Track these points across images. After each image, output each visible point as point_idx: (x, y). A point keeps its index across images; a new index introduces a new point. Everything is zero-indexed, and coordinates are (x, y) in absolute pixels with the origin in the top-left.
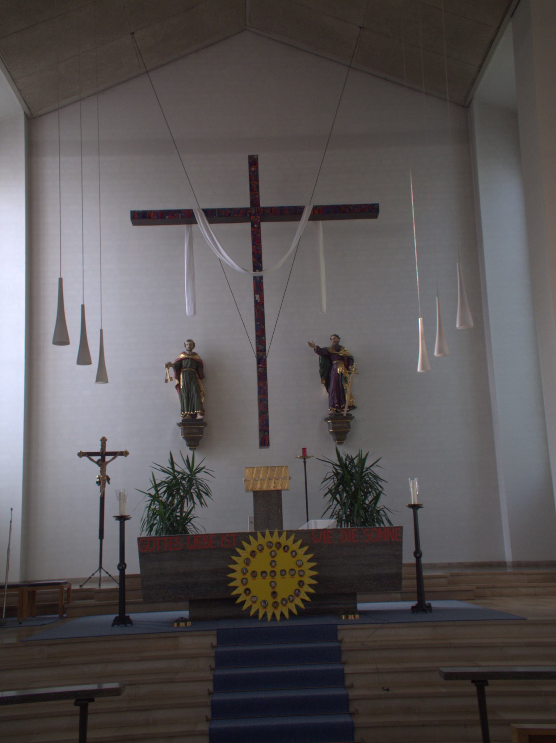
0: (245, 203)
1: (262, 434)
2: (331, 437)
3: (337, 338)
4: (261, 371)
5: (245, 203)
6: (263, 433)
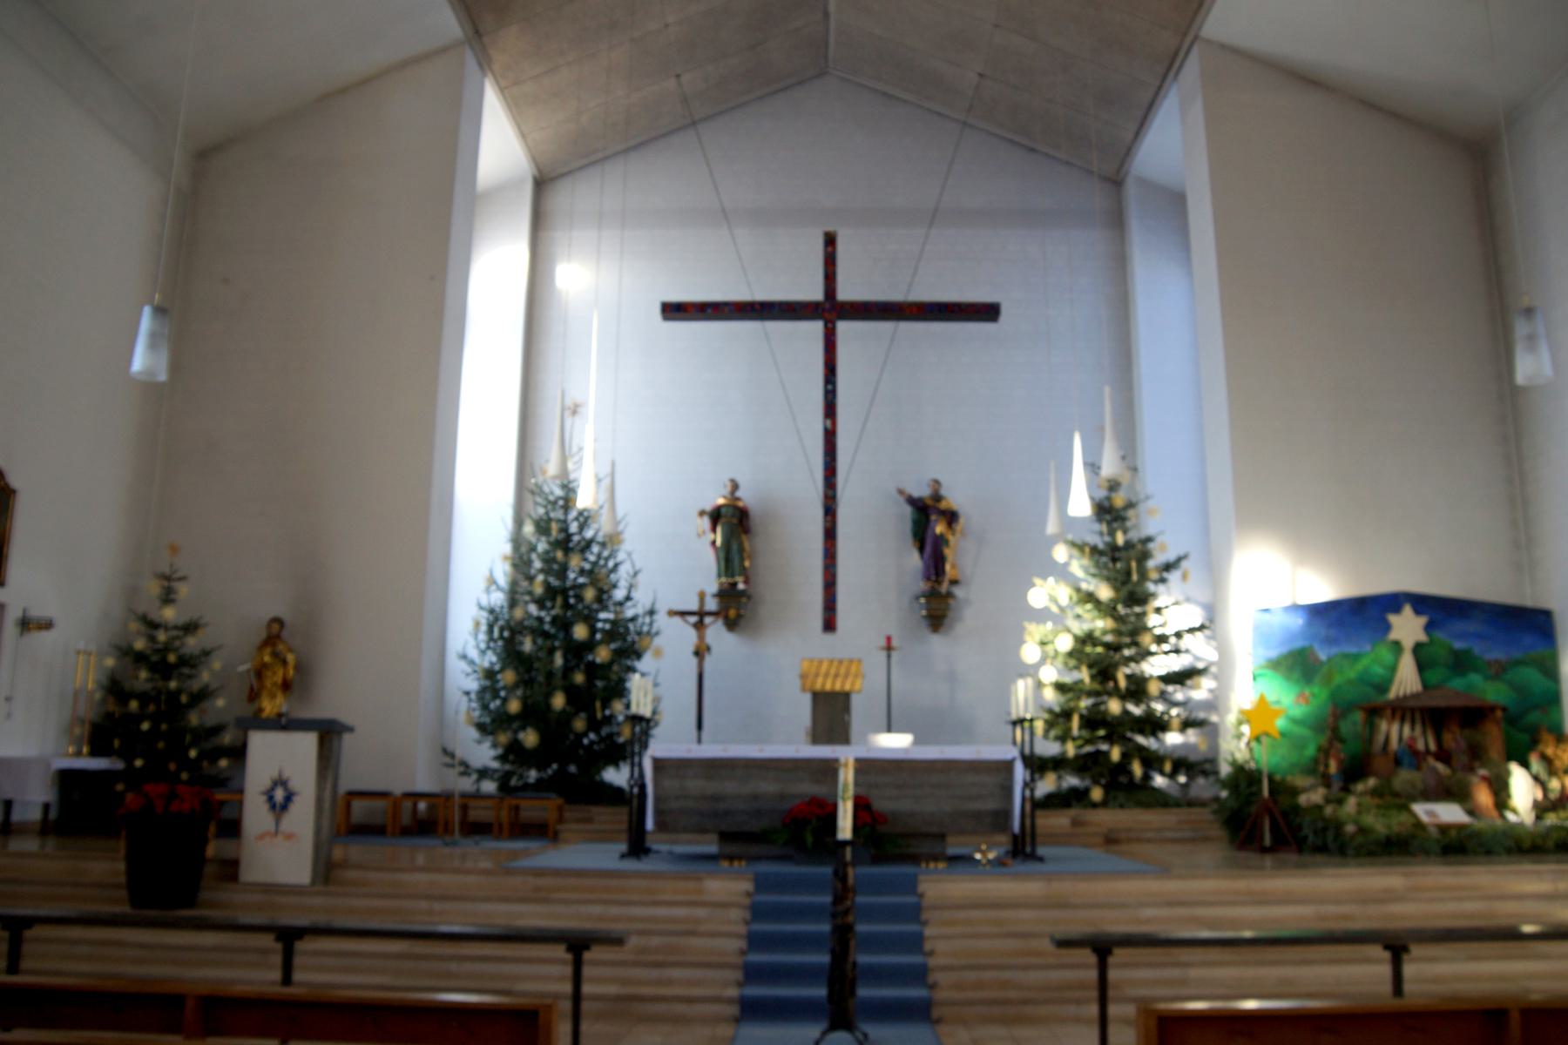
0: (816, 293)
2: (924, 623)
3: (937, 486)
5: (816, 293)
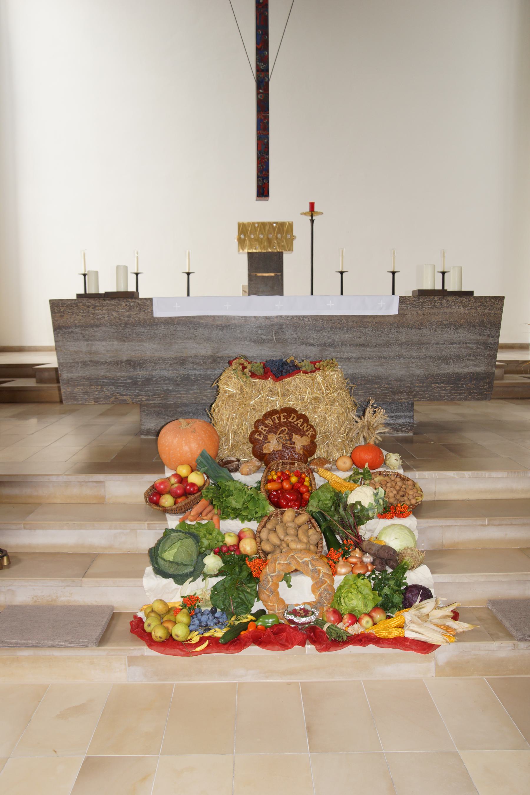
1: (260, 181)
4: (261, 98)
6: (261, 180)
